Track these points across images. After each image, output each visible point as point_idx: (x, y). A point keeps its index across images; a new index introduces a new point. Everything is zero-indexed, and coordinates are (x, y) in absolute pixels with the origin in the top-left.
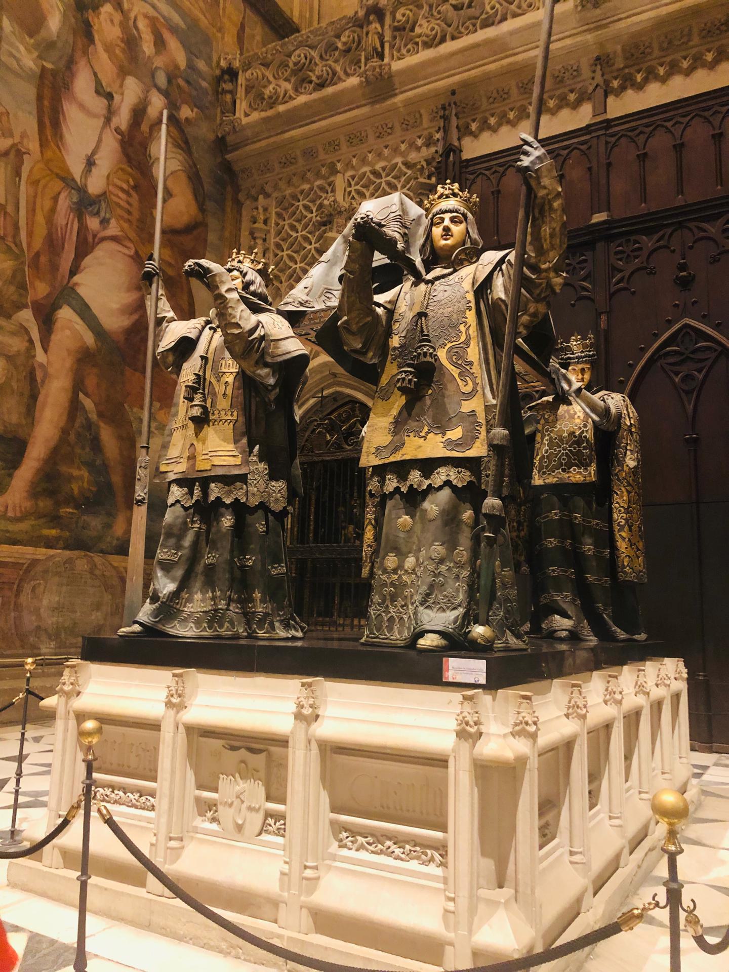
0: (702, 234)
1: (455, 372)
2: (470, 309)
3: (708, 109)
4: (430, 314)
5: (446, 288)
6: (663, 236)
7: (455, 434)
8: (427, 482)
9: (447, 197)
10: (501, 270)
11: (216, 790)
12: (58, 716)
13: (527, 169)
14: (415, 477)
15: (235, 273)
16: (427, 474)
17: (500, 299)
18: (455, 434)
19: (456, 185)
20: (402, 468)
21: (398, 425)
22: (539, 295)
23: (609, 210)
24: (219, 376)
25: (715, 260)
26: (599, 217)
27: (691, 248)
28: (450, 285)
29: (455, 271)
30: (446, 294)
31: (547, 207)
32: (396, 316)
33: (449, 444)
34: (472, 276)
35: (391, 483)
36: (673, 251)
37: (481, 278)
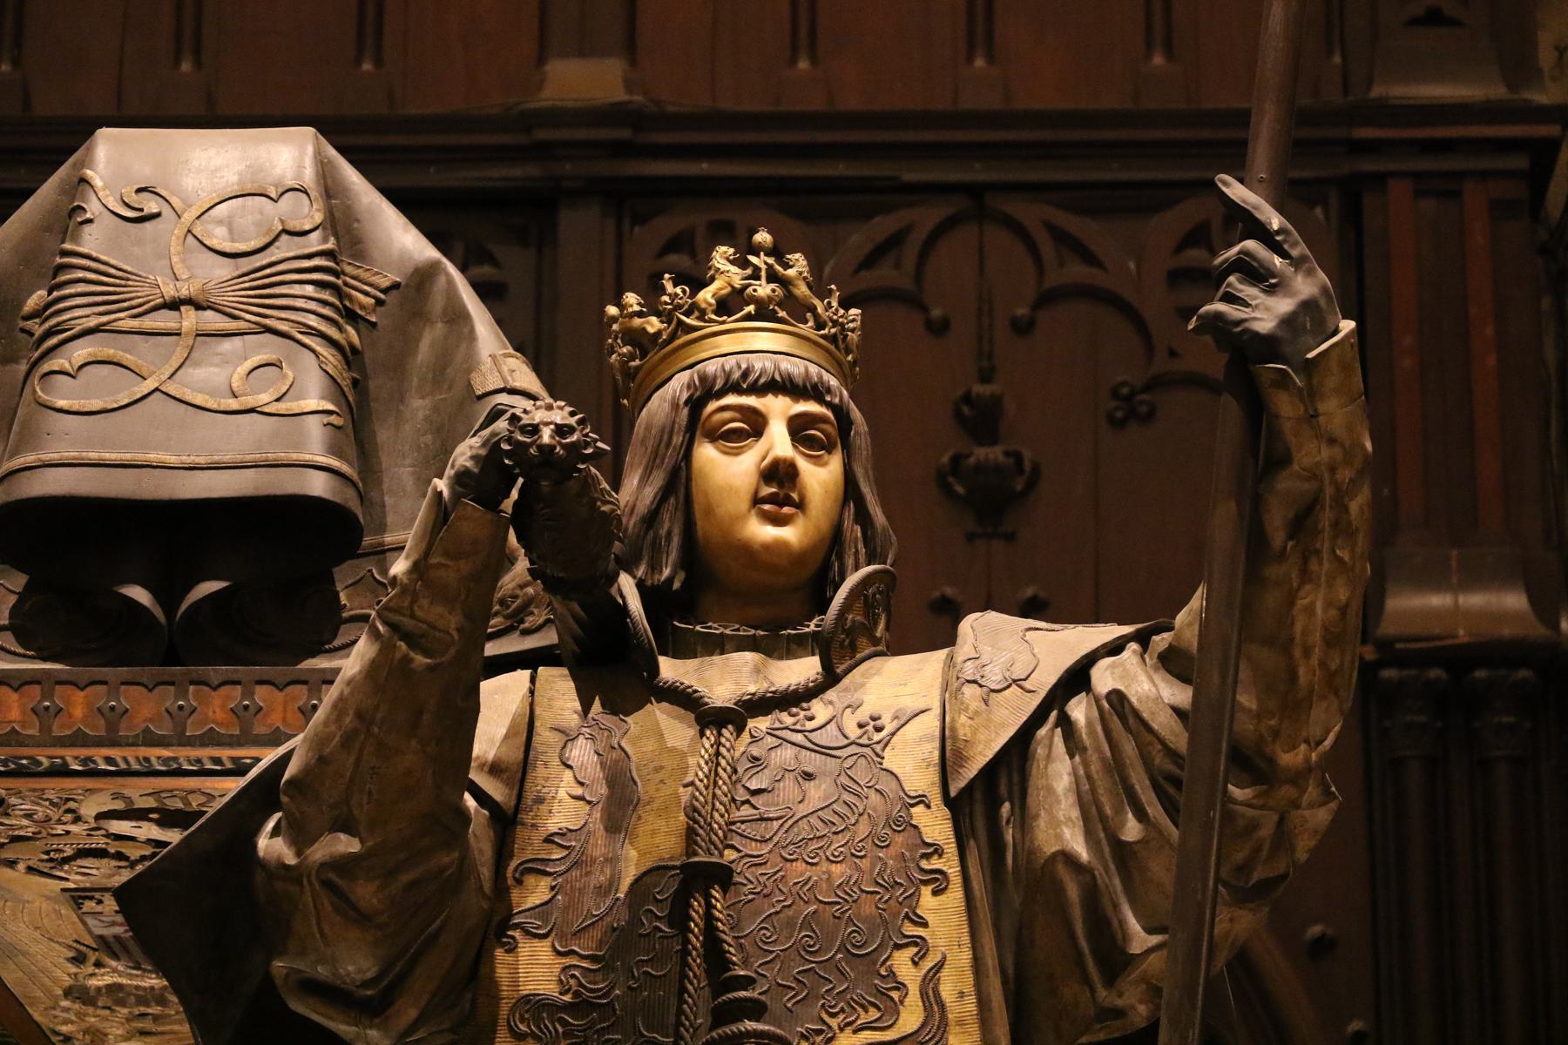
0: (1077, 272)
2: (939, 883)
4: (746, 876)
5: (812, 762)
6: (894, 242)
9: (764, 312)
10: (1065, 722)
13: (1268, 346)
17: (1068, 858)
19: (798, 265)
22: (1243, 869)
23: (630, 49)
25: (1130, 410)
26: (584, 80)
27: (1023, 328)
28: (824, 750)
29: (830, 678)
30: (817, 793)
31: (1326, 517)
32: (528, 846)
34: (930, 723)
36: (939, 328)
37: (986, 747)
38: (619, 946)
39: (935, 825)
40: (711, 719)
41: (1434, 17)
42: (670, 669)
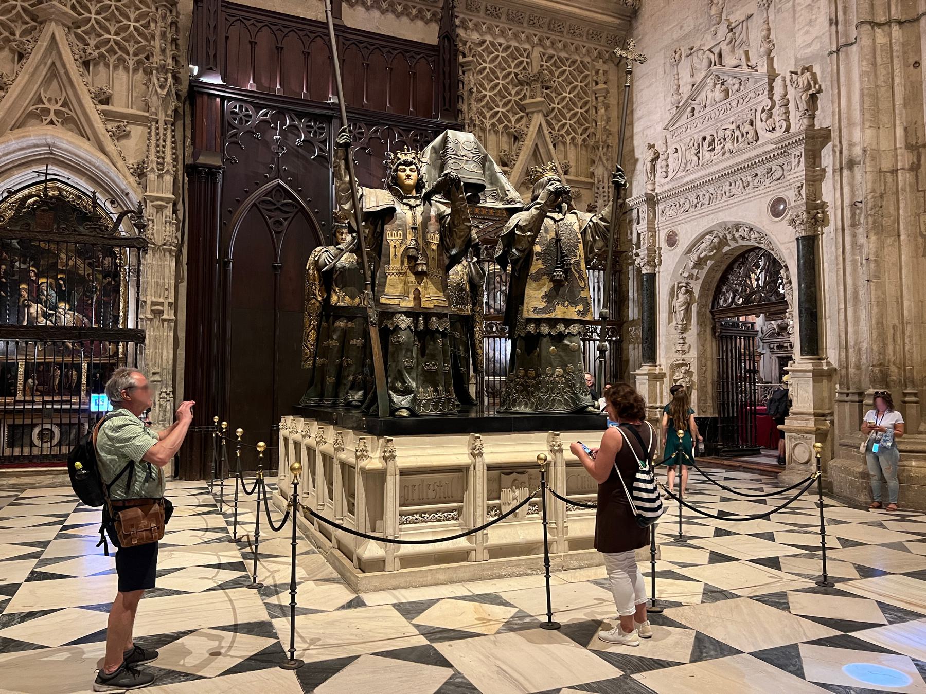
1: (577, 275)
3: (408, 52)
7: (580, 307)
8: (567, 331)
11: (499, 498)
12: (388, 474)
14: (561, 327)
15: (413, 166)
16: (567, 327)
18: (580, 307)
20: (553, 322)
21: (550, 298)
24: (428, 244)
33: (579, 312)
34: (577, 224)
35: (545, 329)
38: (548, 246)
39: (579, 236)
40: (556, 221)
41: (447, 110)
42: (548, 214)
